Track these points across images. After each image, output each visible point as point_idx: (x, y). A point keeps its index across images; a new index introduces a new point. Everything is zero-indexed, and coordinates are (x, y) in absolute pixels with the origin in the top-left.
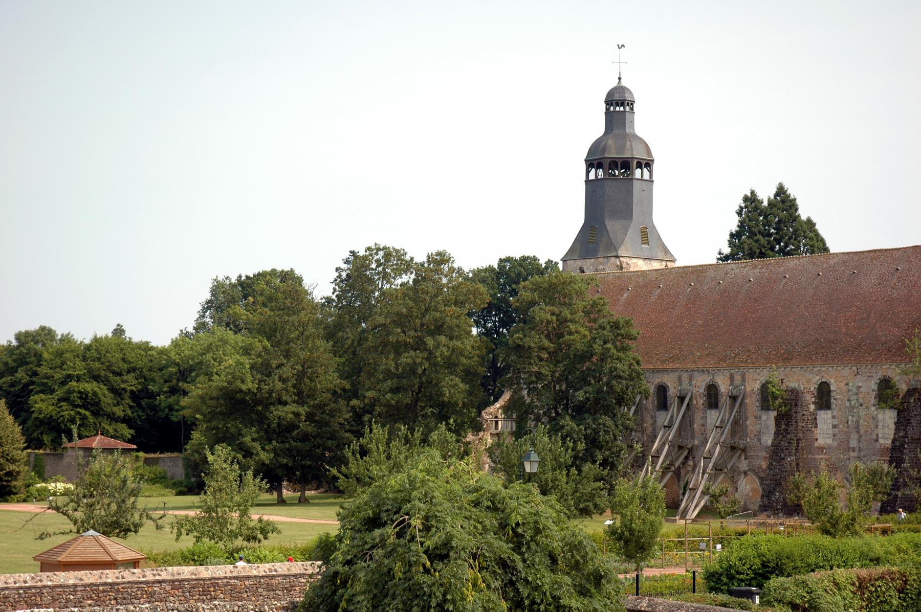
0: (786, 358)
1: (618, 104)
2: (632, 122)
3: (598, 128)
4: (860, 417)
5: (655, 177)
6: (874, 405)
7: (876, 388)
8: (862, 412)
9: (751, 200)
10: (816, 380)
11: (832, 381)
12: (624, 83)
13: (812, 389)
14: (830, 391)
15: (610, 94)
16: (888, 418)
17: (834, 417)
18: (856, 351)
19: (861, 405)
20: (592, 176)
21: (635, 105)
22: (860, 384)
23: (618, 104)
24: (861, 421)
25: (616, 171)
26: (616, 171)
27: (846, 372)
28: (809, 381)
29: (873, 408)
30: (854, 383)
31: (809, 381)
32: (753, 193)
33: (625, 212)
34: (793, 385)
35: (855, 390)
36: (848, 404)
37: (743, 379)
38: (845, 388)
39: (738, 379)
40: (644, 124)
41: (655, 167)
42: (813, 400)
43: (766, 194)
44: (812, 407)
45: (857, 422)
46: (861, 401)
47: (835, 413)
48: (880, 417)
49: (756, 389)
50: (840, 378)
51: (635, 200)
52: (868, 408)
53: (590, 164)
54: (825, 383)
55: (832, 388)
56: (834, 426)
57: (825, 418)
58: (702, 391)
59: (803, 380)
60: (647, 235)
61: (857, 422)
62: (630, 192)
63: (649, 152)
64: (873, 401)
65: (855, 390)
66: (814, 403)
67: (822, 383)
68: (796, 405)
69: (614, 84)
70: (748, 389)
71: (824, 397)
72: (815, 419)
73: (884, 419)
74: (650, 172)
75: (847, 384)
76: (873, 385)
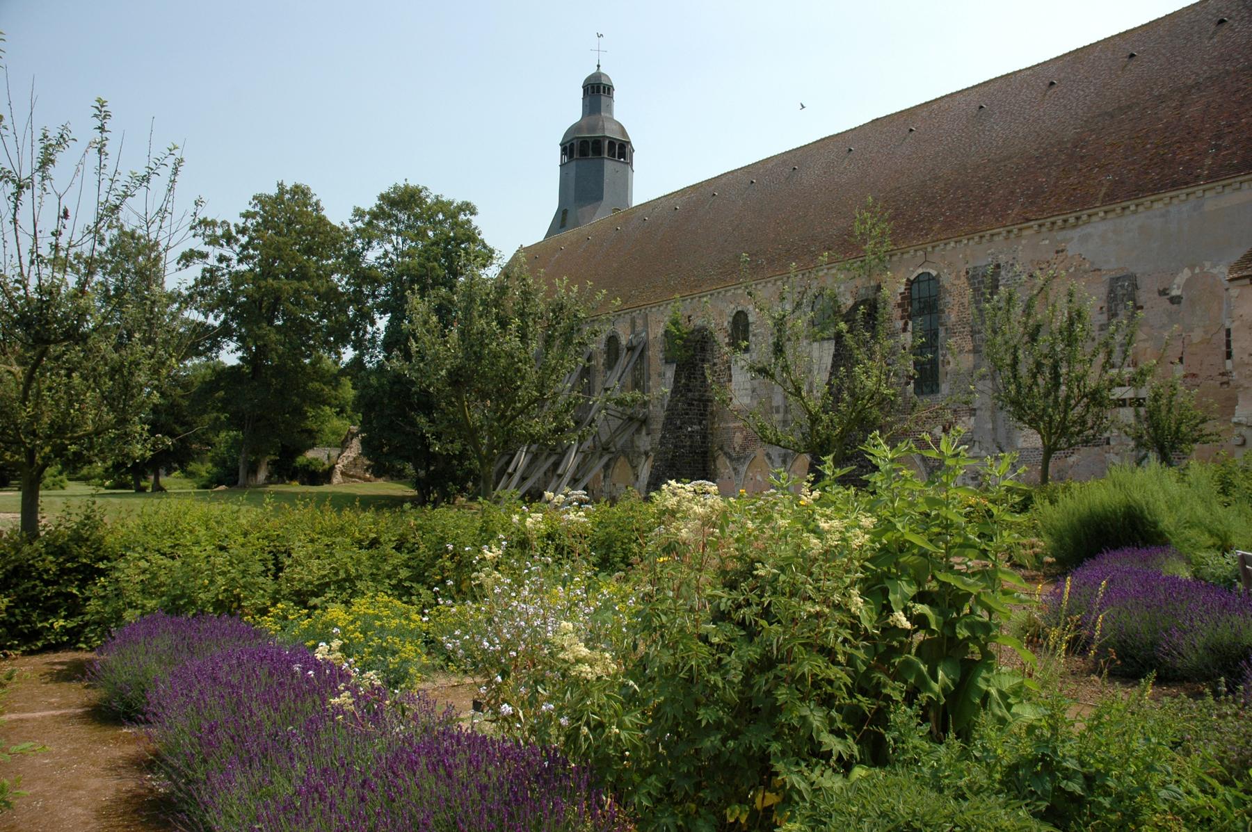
1: (597, 91)
3: (572, 112)
10: (731, 309)
11: (751, 307)
12: (602, 70)
14: (747, 324)
23: (597, 91)
37: (646, 325)
40: (625, 111)
42: (727, 340)
50: (765, 303)
51: (606, 180)
54: (742, 312)
55: (751, 319)
58: (602, 346)
59: (713, 314)
67: (738, 312)
68: (703, 349)
69: (594, 70)
72: (729, 368)
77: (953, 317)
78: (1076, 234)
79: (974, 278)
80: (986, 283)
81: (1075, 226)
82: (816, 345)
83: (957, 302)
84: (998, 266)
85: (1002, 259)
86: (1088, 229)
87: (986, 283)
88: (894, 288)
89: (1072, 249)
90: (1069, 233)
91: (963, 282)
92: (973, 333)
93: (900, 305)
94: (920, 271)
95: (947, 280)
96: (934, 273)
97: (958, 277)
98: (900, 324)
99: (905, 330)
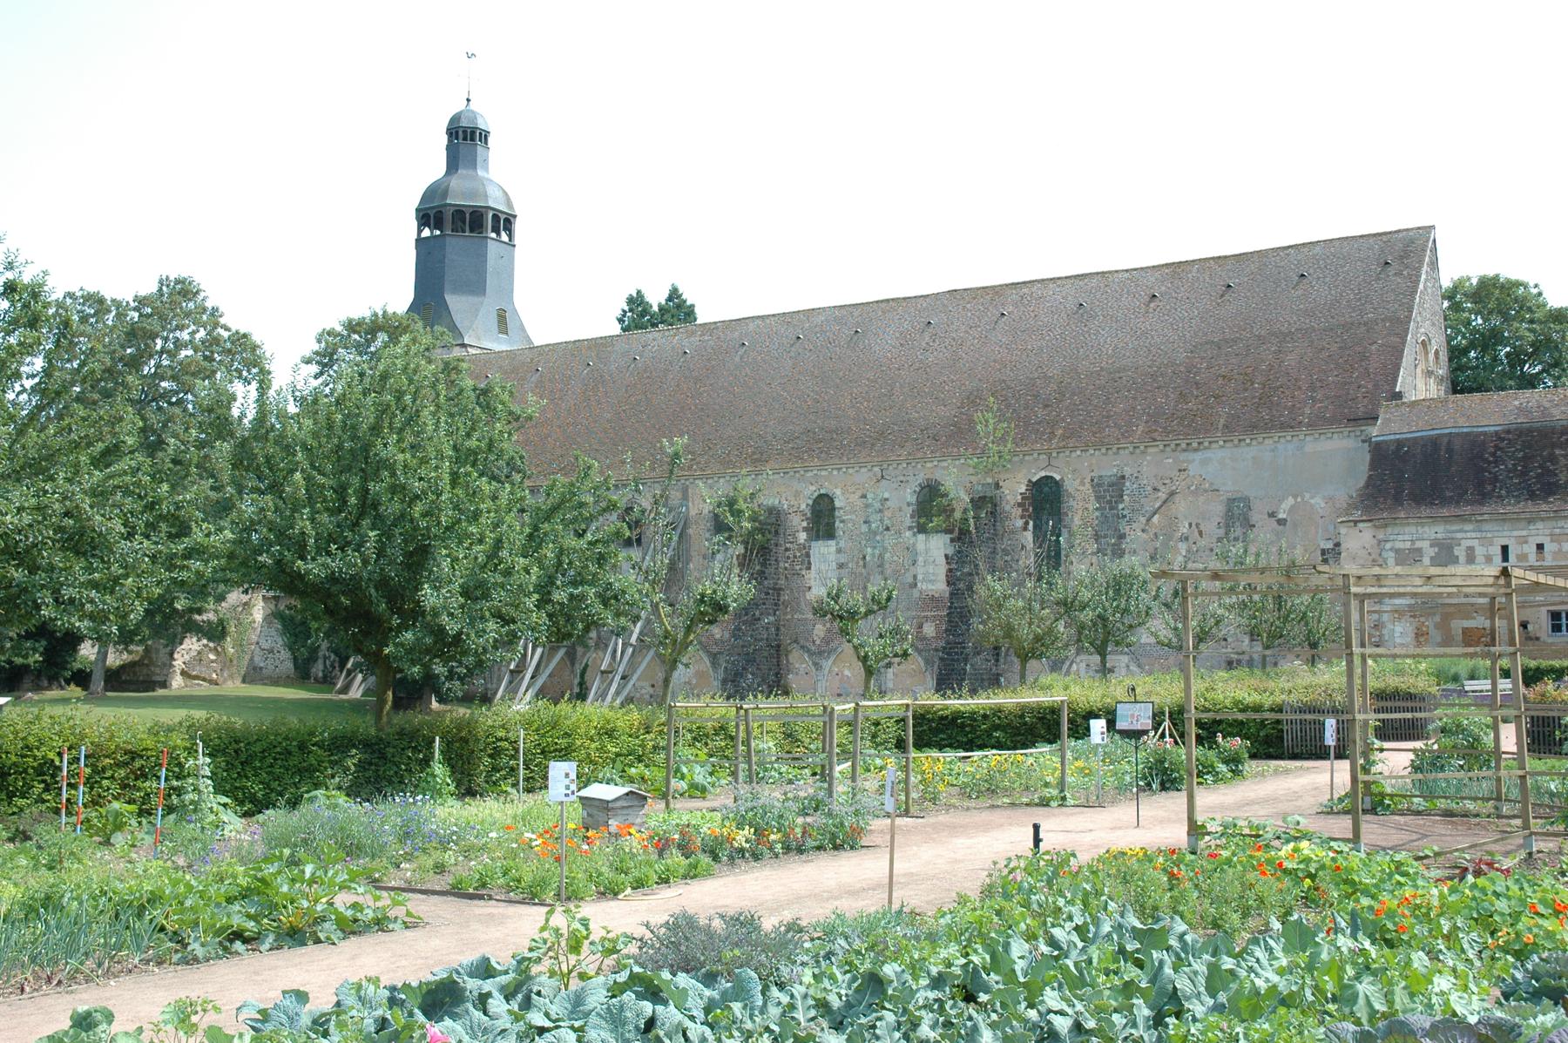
0: (758, 459)
1: (465, 139)
2: (486, 160)
4: (885, 549)
5: (516, 241)
6: (910, 528)
7: (913, 499)
8: (889, 540)
9: (636, 302)
10: (810, 491)
11: (838, 492)
12: (472, 106)
13: (803, 506)
14: (834, 509)
15: (455, 119)
16: (935, 549)
17: (839, 551)
18: (877, 441)
19: (888, 529)
20: (426, 233)
21: (490, 139)
22: (886, 495)
23: (465, 139)
24: (887, 555)
25: (458, 228)
26: (458, 228)
27: (863, 476)
28: (797, 494)
29: (908, 534)
30: (873, 495)
31: (797, 494)
32: (639, 292)
33: (476, 285)
34: (770, 501)
35: (877, 505)
36: (864, 528)
37: (685, 497)
38: (860, 503)
39: (675, 496)
41: (518, 226)
42: (805, 524)
43: (656, 298)
44: (802, 537)
45: (881, 556)
46: (887, 522)
47: (842, 544)
48: (920, 546)
49: (706, 512)
51: (490, 269)
52: (899, 533)
53: (427, 216)
55: (837, 504)
56: (841, 566)
57: (824, 553)
59: (790, 495)
60: (503, 321)
61: (881, 556)
62: (482, 257)
63: (509, 203)
64: (908, 522)
65: (877, 505)
66: (805, 529)
67: (821, 496)
68: (777, 533)
70: (693, 512)
71: (823, 518)
72: (808, 555)
73: (927, 551)
74: (510, 236)
75: (864, 496)
76: (909, 495)
77: (1077, 521)
78: (1198, 456)
79: (1096, 484)
80: (1111, 492)
81: (1196, 450)
82: (921, 537)
83: (1081, 508)
84: (1123, 477)
85: (1127, 471)
86: (1208, 454)
87: (1111, 492)
88: (1014, 488)
89: (1194, 469)
90: (1191, 456)
91: (1087, 489)
92: (1097, 537)
93: (1019, 505)
94: (1043, 474)
95: (1070, 485)
96: (1058, 478)
97: (1082, 483)
98: (1020, 523)
99: (1025, 529)
